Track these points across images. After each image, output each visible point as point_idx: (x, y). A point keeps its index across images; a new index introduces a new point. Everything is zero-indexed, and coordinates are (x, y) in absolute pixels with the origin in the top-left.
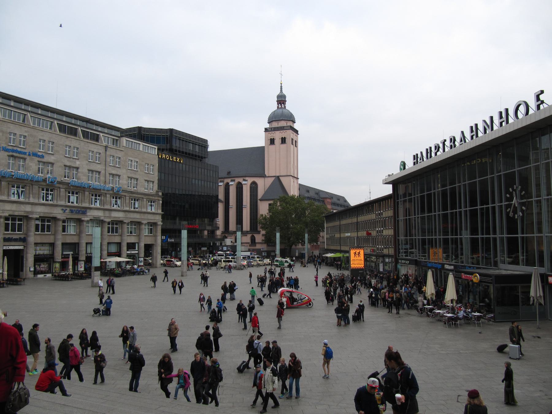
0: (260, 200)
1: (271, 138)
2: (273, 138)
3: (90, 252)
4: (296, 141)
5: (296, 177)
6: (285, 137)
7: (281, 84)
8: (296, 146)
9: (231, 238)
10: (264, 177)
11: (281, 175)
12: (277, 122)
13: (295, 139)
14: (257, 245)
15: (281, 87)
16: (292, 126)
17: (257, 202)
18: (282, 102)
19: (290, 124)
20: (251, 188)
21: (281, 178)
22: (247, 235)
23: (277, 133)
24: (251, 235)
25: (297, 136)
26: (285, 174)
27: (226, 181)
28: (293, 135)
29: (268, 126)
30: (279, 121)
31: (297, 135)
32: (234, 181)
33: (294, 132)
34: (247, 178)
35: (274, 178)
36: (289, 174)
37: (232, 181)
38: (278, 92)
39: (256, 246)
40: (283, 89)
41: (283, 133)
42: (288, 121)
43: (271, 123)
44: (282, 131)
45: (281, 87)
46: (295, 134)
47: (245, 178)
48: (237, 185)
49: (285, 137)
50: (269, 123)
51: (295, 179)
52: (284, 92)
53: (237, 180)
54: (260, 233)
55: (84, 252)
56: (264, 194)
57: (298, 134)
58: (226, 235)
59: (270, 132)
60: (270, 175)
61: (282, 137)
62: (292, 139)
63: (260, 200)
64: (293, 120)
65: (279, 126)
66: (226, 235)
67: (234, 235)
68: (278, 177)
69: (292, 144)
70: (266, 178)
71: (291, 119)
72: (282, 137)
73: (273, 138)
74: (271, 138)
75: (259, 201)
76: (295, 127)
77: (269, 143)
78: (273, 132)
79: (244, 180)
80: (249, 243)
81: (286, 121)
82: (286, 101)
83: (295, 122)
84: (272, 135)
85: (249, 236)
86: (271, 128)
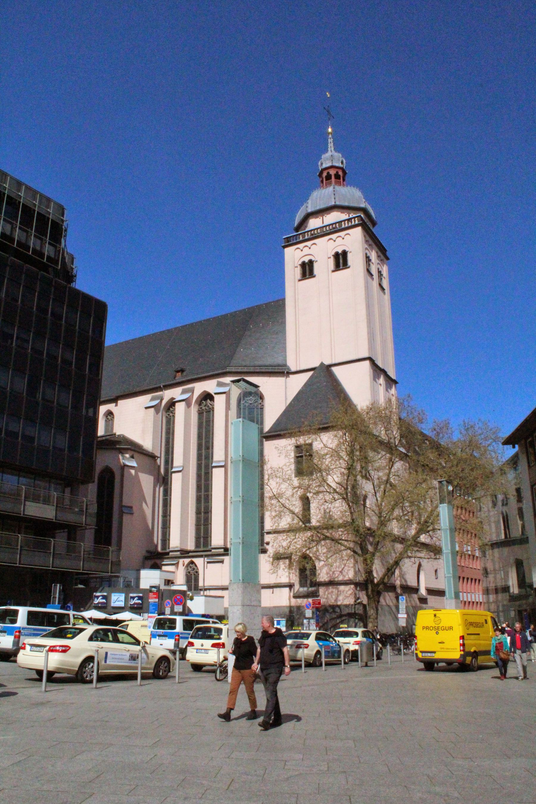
10: (283, 373)
21: (335, 369)
22: (222, 562)
65: (326, 223)
78: (309, 243)
84: (306, 251)
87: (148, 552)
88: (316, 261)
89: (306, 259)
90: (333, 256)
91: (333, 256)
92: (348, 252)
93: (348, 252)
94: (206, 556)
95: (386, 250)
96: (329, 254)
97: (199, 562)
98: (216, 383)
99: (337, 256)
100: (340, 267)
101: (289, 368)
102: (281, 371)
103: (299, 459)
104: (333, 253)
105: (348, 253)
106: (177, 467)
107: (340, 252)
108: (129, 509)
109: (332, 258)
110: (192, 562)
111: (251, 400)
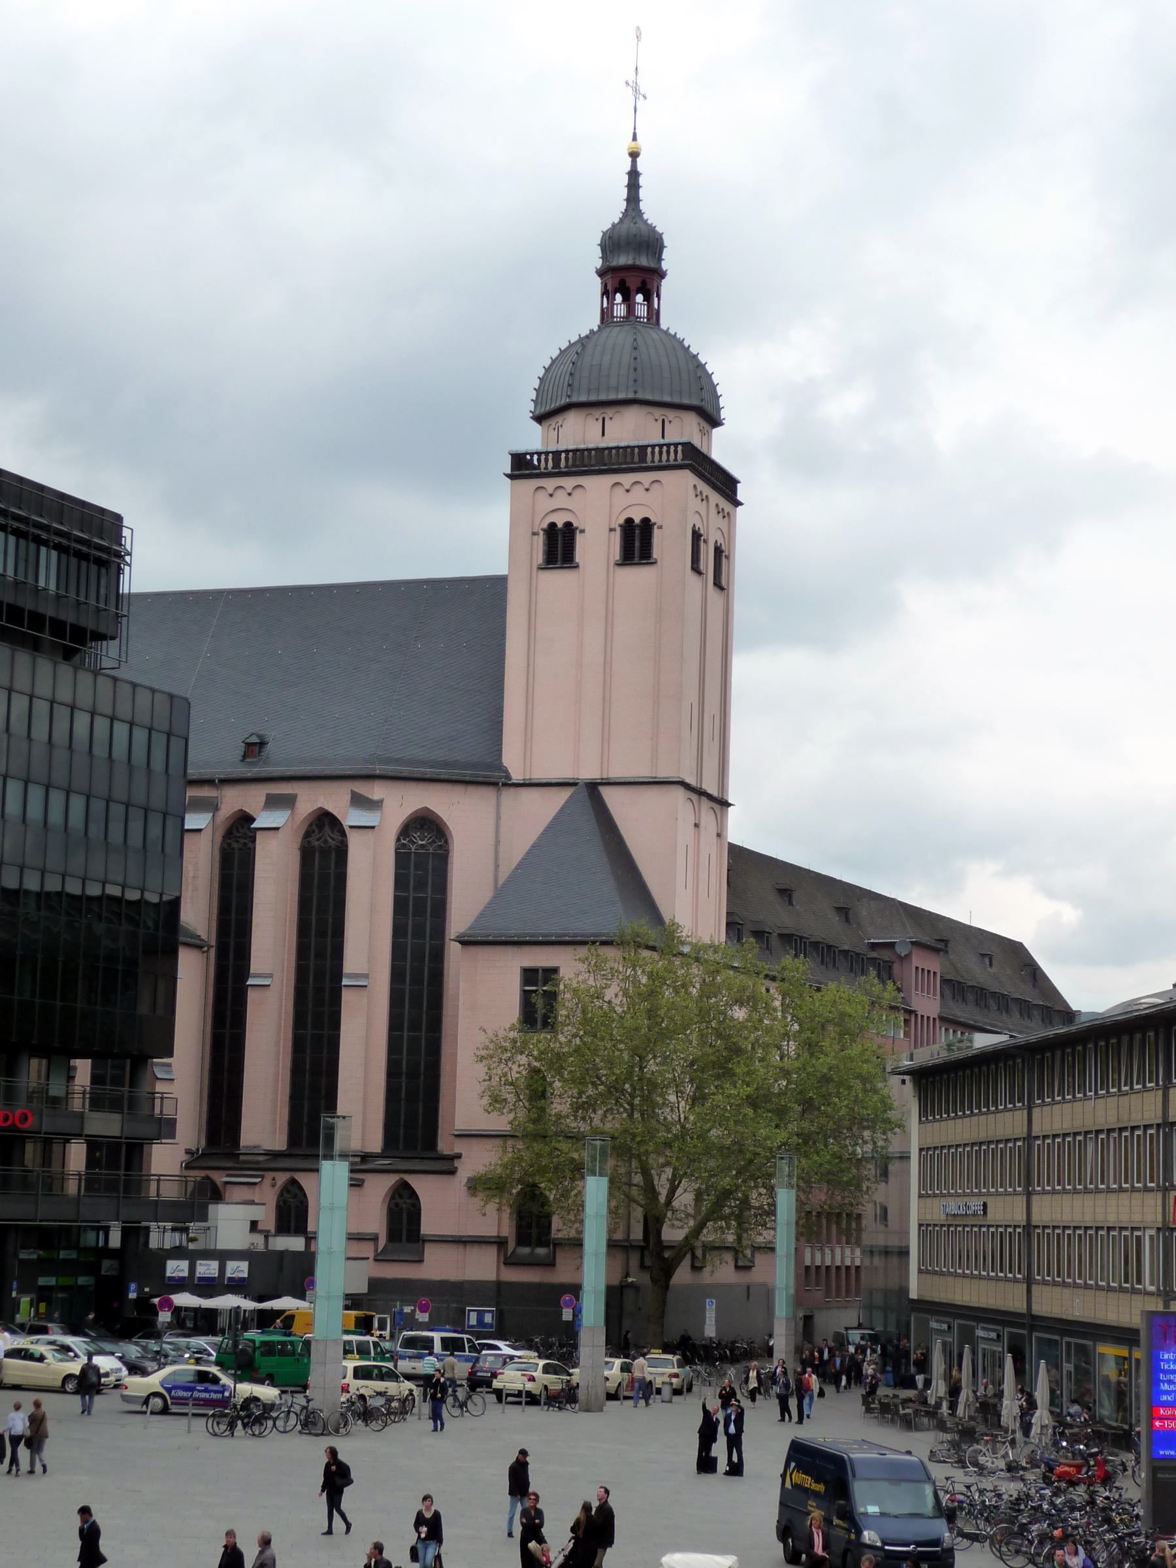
0: (466, 942)
1: (553, 525)
2: (568, 525)
4: (718, 551)
5: (714, 792)
7: (634, 155)
8: (718, 584)
9: (252, 1203)
10: (495, 784)
11: (615, 773)
12: (598, 413)
13: (713, 537)
14: (432, 1253)
15: (634, 175)
16: (697, 443)
17: (438, 956)
18: (633, 282)
19: (684, 428)
20: (402, 858)
23: (597, 486)
24: (390, 1181)
25: (728, 516)
26: (642, 771)
27: (233, 800)
28: (702, 508)
29: (533, 438)
30: (609, 412)
32: (287, 802)
33: (715, 487)
34: (376, 791)
36: (663, 773)
37: (273, 802)
38: (613, 210)
39: (421, 1261)
40: (642, 193)
41: (638, 494)
42: (670, 414)
43: (553, 422)
44: (627, 479)
45: (634, 175)
46: (715, 498)
47: (362, 788)
48: (307, 835)
49: (646, 522)
50: (540, 419)
51: (705, 804)
52: (652, 211)
53: (311, 798)
54: (452, 1172)
56: (491, 903)
57: (737, 504)
58: (220, 1178)
59: (550, 484)
60: (539, 775)
61: (629, 521)
62: (696, 536)
63: (466, 942)
64: (709, 408)
66: (220, 1178)
67: (269, 1175)
68: (593, 788)
69: (696, 568)
70: (508, 795)
71: (695, 402)
72: (629, 521)
73: (568, 525)
74: (553, 525)
75: (453, 950)
76: (717, 455)
77: (540, 558)
78: (569, 482)
79: (359, 801)
80: (374, 1238)
81: (659, 413)
82: (662, 275)
83: (713, 420)
86: (557, 454)
87: (188, 1152)
88: (582, 531)
90: (620, 526)
91: (620, 526)
93: (655, 524)
96: (614, 520)
98: (349, 797)
99: (628, 526)
101: (508, 777)
102: (492, 780)
104: (621, 521)
105: (656, 527)
107: (637, 521)
108: (165, 1068)
109: (618, 529)
110: (293, 1182)
111: (420, 840)
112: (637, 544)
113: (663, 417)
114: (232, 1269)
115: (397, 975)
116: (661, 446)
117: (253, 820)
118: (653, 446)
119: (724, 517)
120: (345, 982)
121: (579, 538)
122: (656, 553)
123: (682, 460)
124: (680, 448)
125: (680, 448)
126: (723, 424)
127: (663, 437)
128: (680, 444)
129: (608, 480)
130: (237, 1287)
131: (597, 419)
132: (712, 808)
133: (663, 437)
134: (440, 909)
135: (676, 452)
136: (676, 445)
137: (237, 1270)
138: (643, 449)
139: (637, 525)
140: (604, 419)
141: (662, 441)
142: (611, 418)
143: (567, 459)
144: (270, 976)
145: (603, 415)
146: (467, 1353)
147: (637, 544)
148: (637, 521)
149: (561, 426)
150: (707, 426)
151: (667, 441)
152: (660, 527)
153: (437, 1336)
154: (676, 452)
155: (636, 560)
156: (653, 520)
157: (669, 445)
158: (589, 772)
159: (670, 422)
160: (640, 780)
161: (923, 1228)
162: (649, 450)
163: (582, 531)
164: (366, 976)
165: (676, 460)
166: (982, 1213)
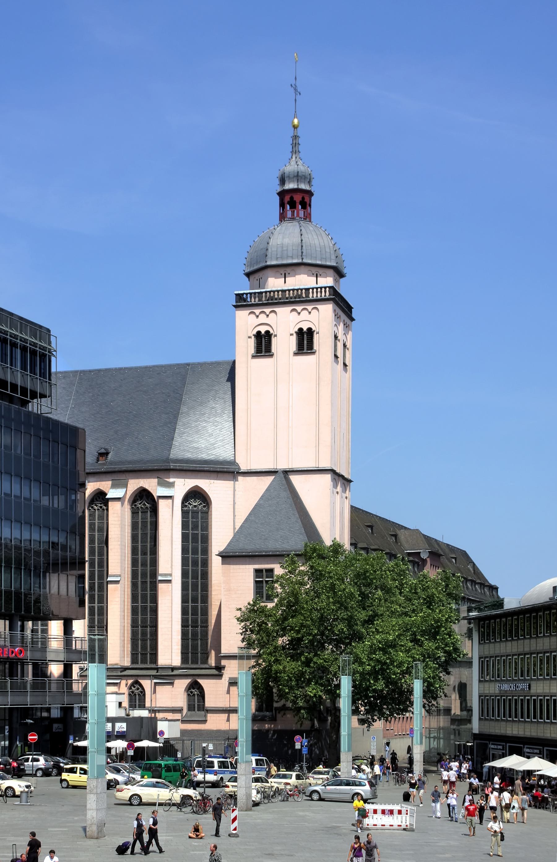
3: (431, 739)
6: (310, 329)
21: (295, 479)
23: (283, 311)
24: (186, 682)
31: (347, 320)
35: (270, 479)
43: (257, 276)
44: (299, 308)
49: (310, 329)
55: (415, 739)
61: (301, 330)
68: (286, 473)
72: (301, 330)
74: (259, 333)
75: (216, 562)
84: (263, 319)
85: (182, 684)
89: (263, 329)
90: (296, 332)
91: (296, 332)
92: (314, 331)
93: (314, 331)
94: (156, 677)
95: (350, 308)
97: (147, 684)
99: (300, 332)
100: (303, 350)
101: (239, 468)
103: (258, 585)
105: (315, 333)
106: (114, 576)
107: (305, 329)
109: (295, 335)
110: (137, 682)
111: (194, 503)
112: (305, 342)
113: (317, 273)
114: (118, 727)
115: (184, 574)
116: (317, 288)
117: (106, 494)
118: (313, 289)
119: (347, 327)
120: (160, 578)
121: (274, 340)
122: (316, 347)
123: (329, 296)
124: (327, 289)
125: (327, 289)
126: (346, 276)
127: (317, 283)
128: (328, 287)
129: (289, 309)
130: (121, 736)
131: (281, 274)
132: (335, 479)
133: (317, 283)
134: (206, 539)
135: (325, 292)
136: (325, 288)
137: (121, 727)
138: (307, 290)
139: (305, 332)
140: (285, 274)
141: (314, 285)
142: (289, 274)
143: (266, 297)
144: (120, 576)
145: (285, 272)
146: (230, 769)
147: (305, 342)
148: (305, 329)
149: (261, 278)
150: (338, 278)
151: (318, 286)
152: (318, 333)
153: (216, 761)
154: (325, 292)
155: (305, 351)
156: (314, 329)
157: (321, 288)
158: (282, 465)
159: (320, 275)
160: (310, 469)
161: (481, 698)
162: (311, 290)
163: (276, 336)
164: (171, 575)
165: (325, 296)
166: (528, 689)
